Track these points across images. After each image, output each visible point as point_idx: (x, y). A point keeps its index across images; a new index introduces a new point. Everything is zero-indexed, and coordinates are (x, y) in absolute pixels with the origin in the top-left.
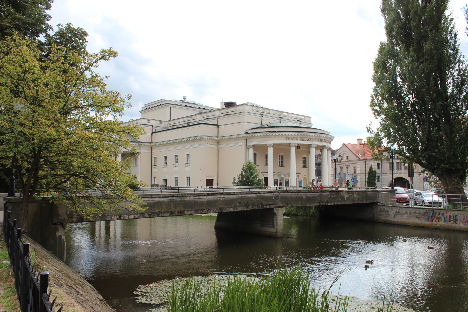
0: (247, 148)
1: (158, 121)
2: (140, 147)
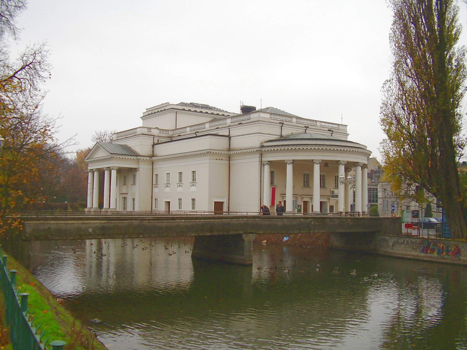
0: (262, 164)
2: (138, 162)
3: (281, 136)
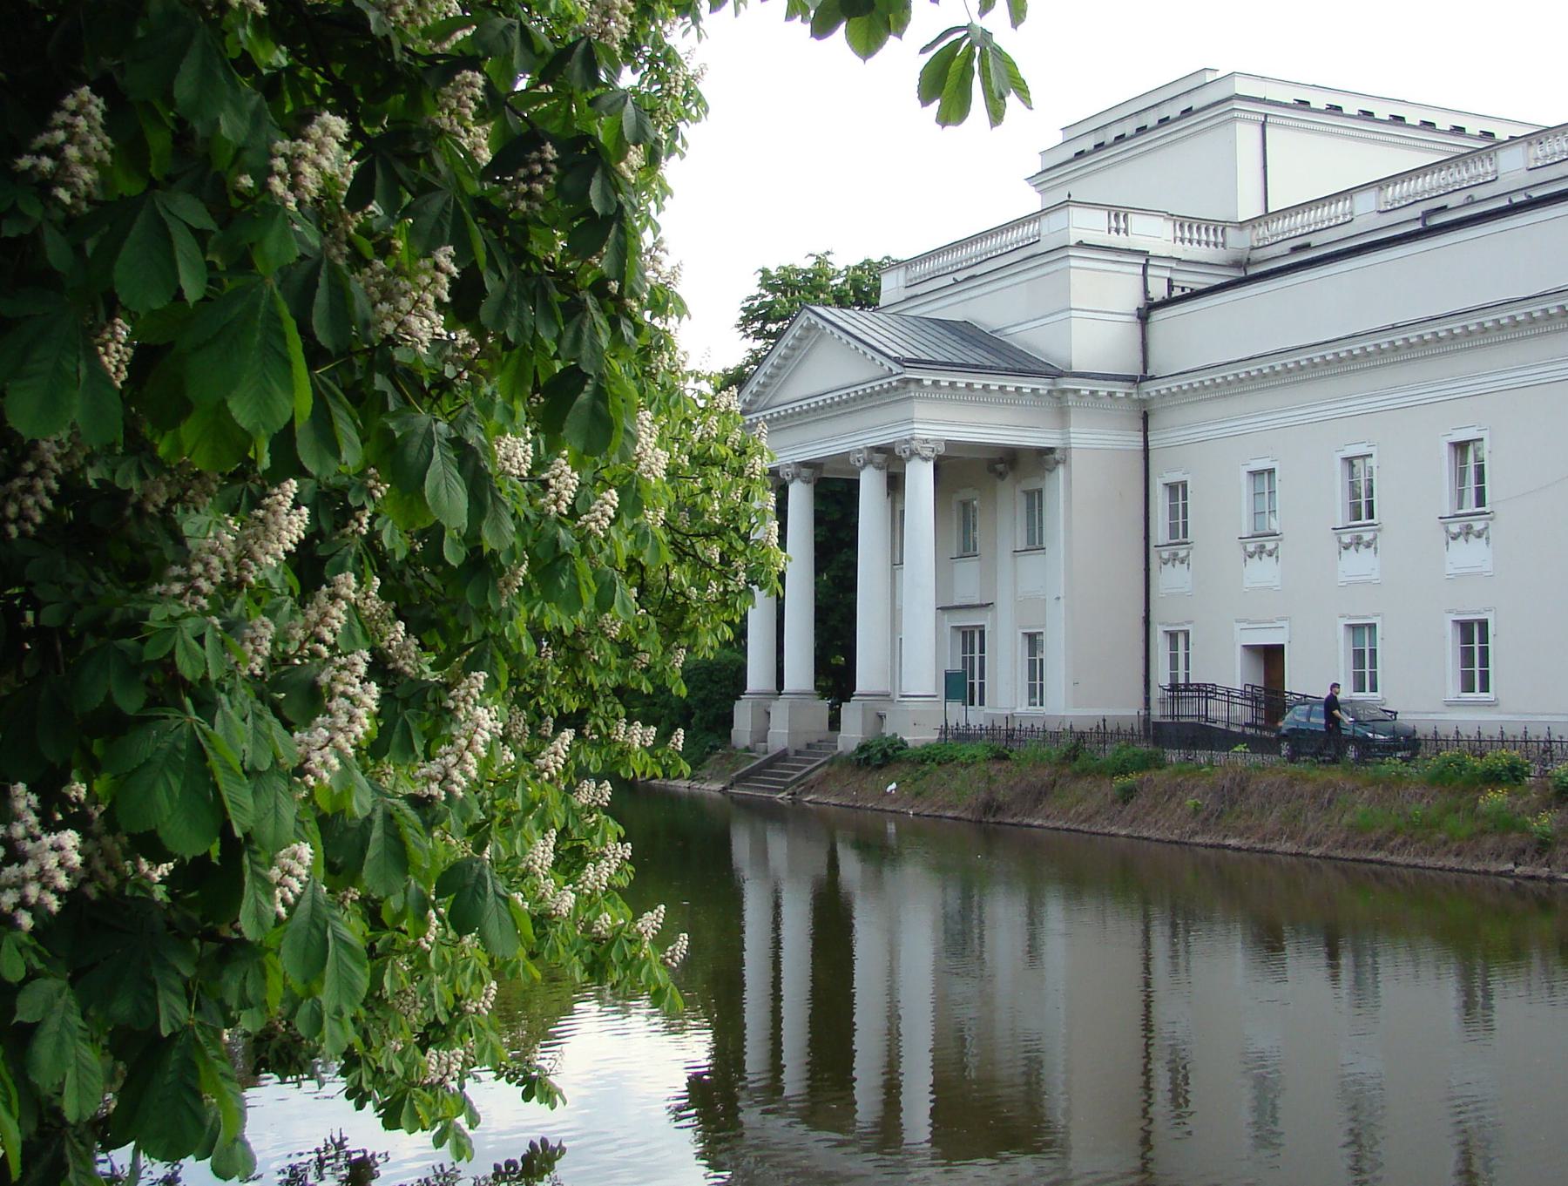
1: (1182, 221)
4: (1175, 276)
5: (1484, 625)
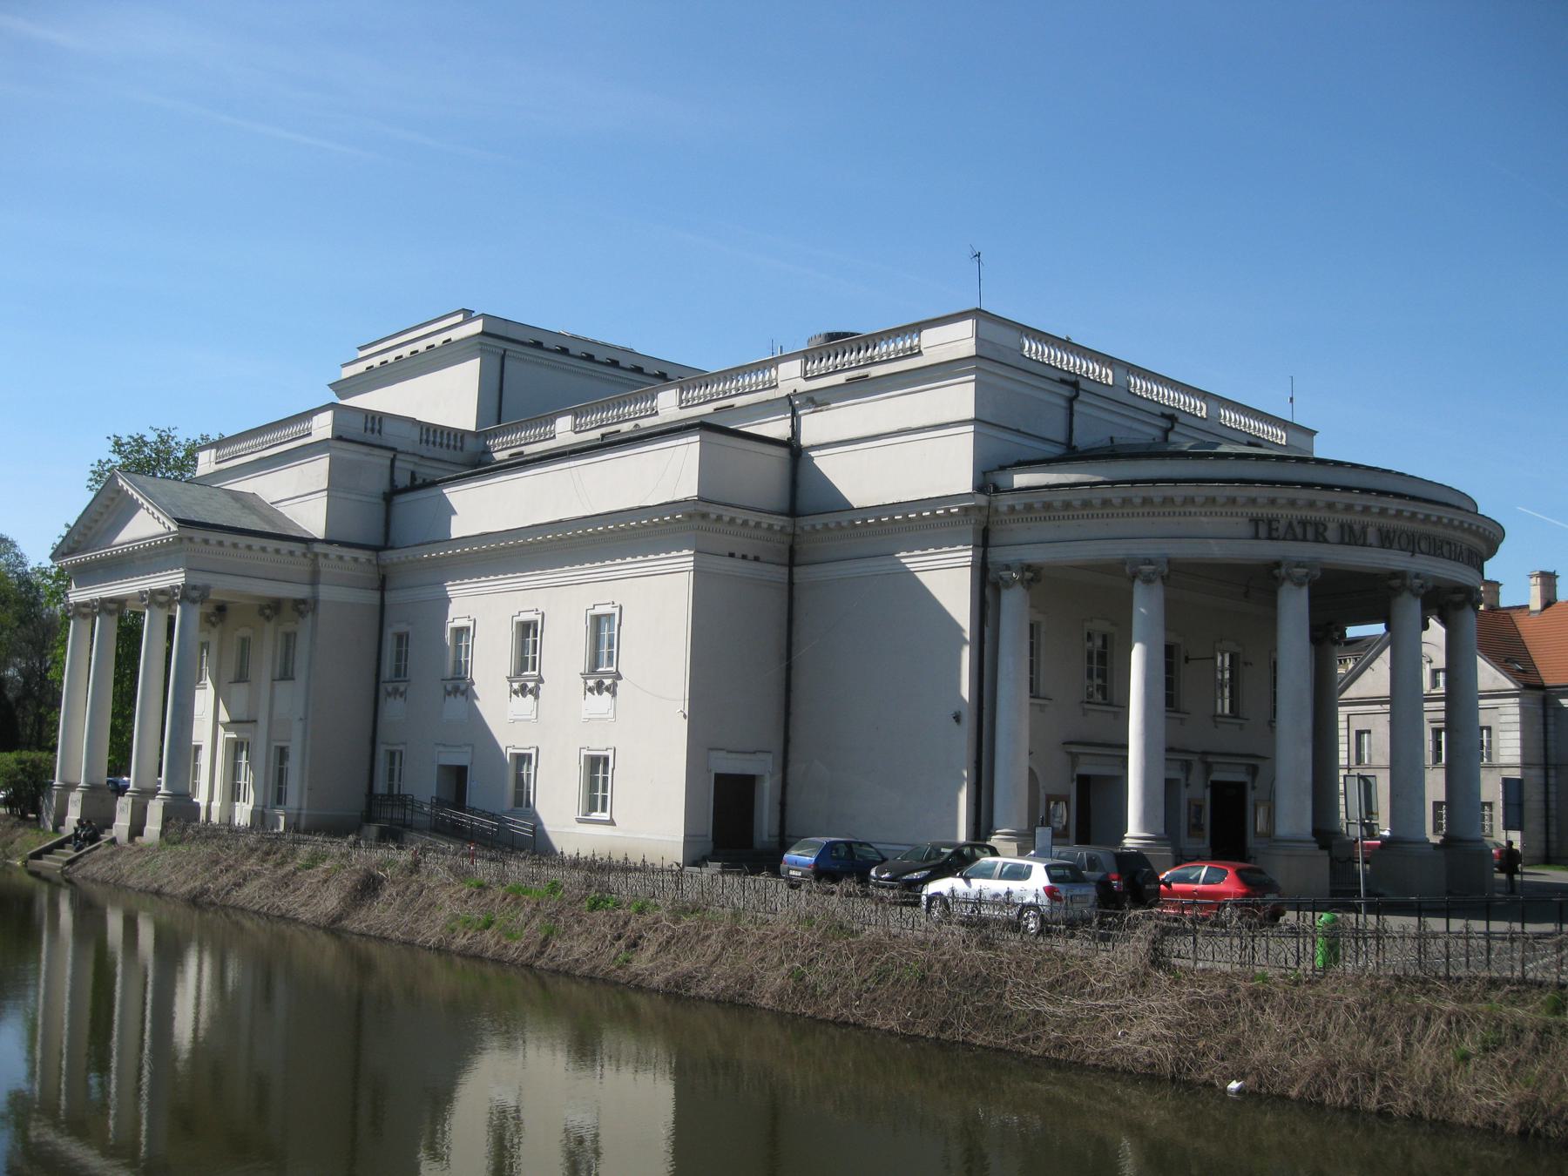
3: (1069, 445)
4: (417, 469)
5: (606, 759)
